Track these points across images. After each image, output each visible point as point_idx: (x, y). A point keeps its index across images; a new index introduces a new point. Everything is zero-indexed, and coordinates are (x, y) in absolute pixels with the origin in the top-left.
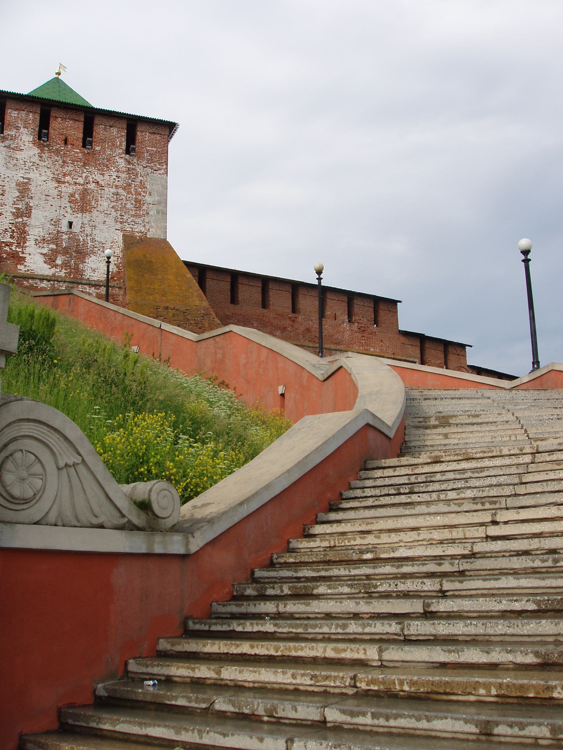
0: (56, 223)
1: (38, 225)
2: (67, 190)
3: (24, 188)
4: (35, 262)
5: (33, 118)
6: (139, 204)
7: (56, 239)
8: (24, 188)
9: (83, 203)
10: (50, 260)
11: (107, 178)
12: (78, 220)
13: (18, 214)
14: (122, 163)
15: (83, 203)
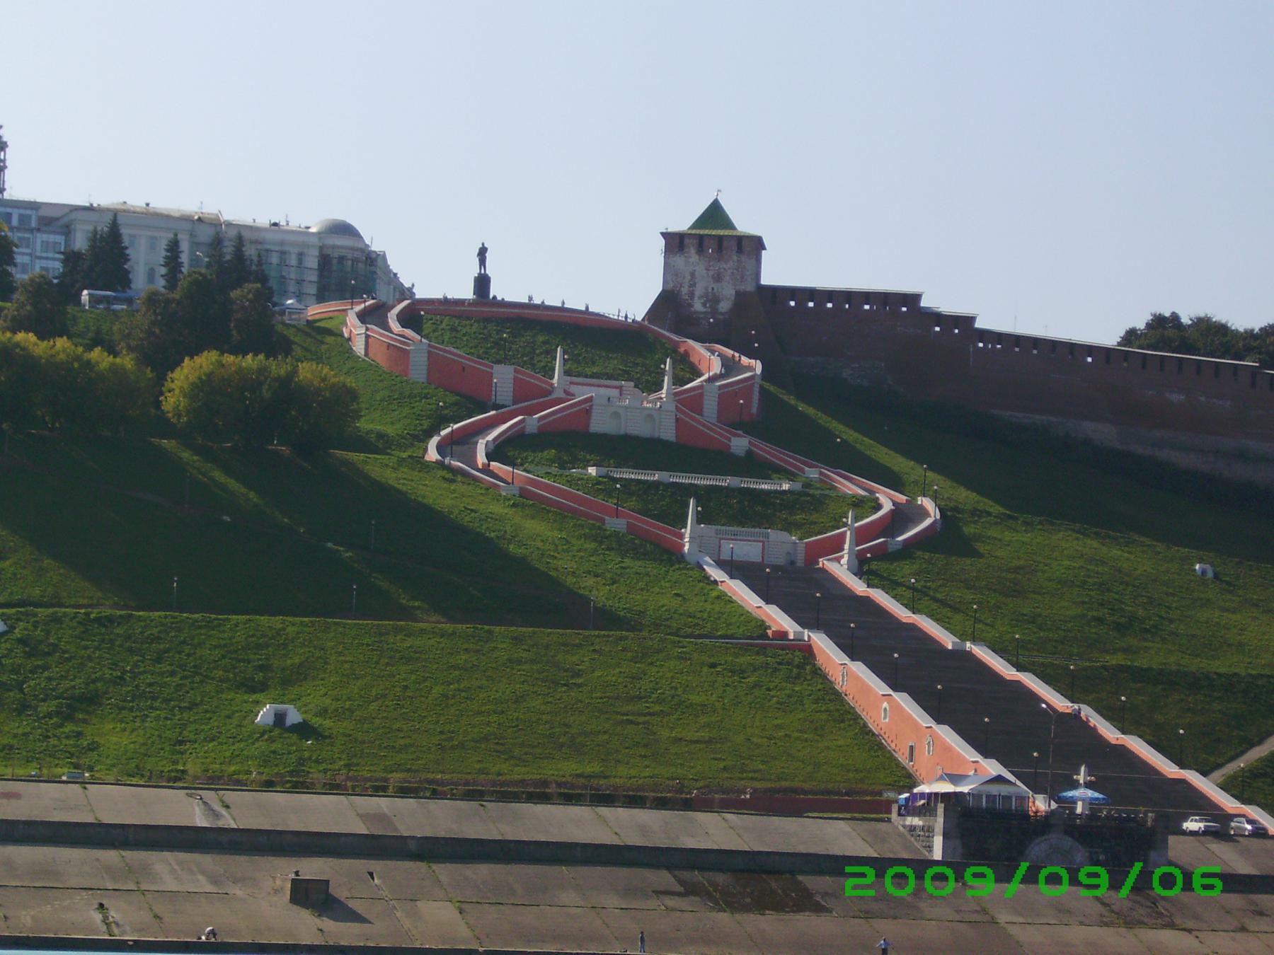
0: (706, 288)
1: (699, 291)
2: (711, 273)
3: (693, 274)
4: (698, 306)
5: (695, 241)
6: (742, 277)
7: (706, 295)
8: (693, 274)
9: (718, 278)
10: (704, 305)
11: (731, 264)
12: (715, 286)
13: (691, 286)
14: (735, 258)
15: (718, 278)
